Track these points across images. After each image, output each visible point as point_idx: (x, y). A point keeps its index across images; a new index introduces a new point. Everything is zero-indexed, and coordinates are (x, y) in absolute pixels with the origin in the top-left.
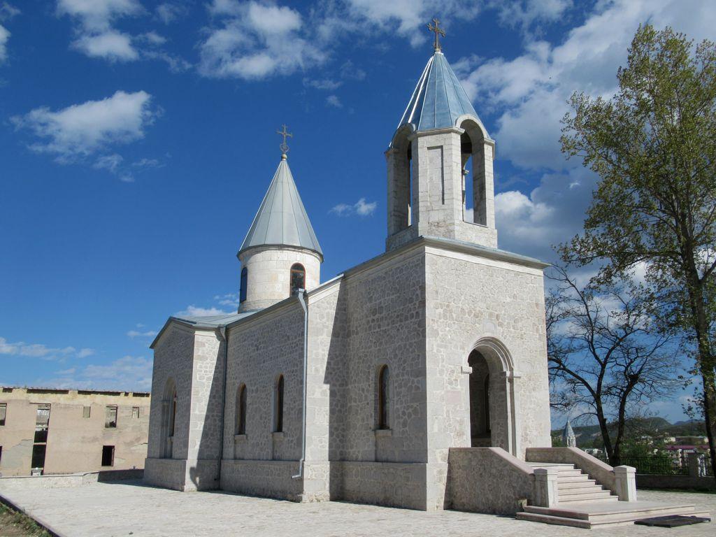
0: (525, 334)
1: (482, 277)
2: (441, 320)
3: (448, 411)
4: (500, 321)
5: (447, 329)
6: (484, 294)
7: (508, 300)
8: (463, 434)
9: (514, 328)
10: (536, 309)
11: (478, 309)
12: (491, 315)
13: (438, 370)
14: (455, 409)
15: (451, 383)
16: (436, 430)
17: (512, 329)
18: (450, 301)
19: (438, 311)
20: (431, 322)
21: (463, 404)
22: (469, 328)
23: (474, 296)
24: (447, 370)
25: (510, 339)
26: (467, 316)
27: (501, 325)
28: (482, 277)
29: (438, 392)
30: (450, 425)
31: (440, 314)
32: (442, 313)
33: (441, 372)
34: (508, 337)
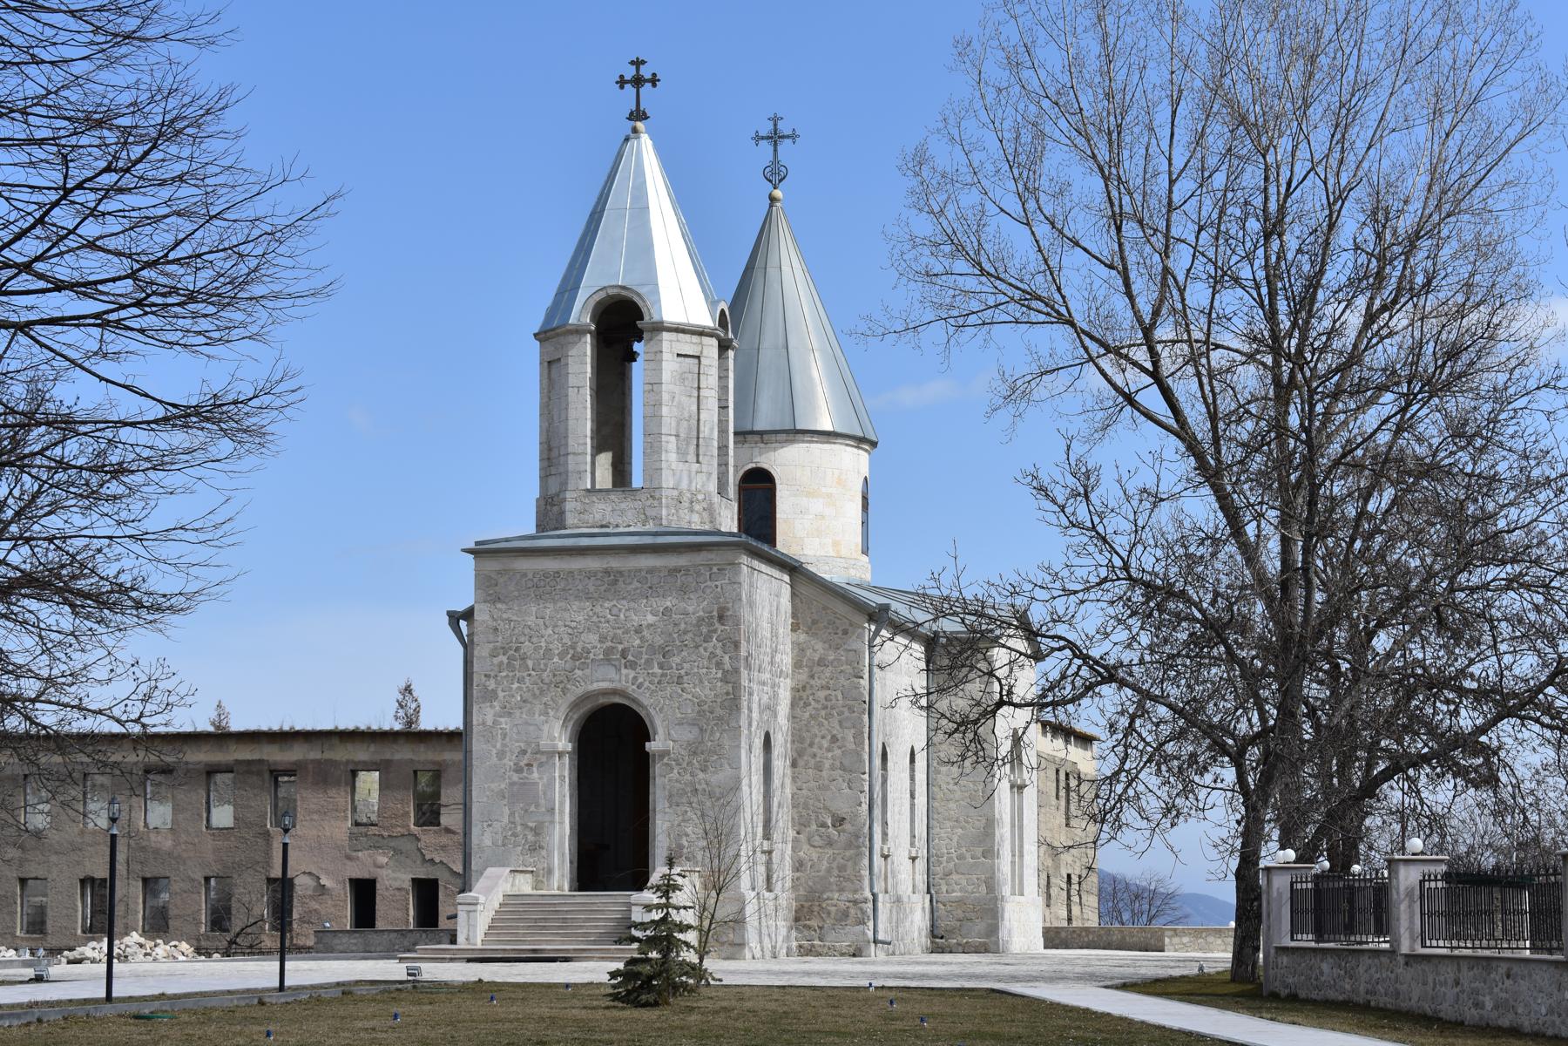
0: (687, 674)
1: (592, 589)
2: (504, 674)
3: (512, 814)
4: (630, 657)
5: (516, 685)
6: (595, 619)
7: (651, 619)
8: (541, 847)
9: (661, 667)
10: (717, 625)
11: (580, 645)
12: (608, 652)
13: (494, 751)
14: (526, 811)
15: (519, 770)
16: (488, 842)
17: (656, 670)
18: (522, 639)
19: (496, 661)
20: (483, 678)
21: (542, 802)
22: (558, 679)
23: (574, 624)
24: (512, 753)
25: (653, 687)
26: (556, 659)
27: (632, 665)
28: (592, 589)
29: (493, 786)
30: (515, 835)
31: (502, 663)
32: (506, 661)
33: (501, 755)
34: (647, 684)
